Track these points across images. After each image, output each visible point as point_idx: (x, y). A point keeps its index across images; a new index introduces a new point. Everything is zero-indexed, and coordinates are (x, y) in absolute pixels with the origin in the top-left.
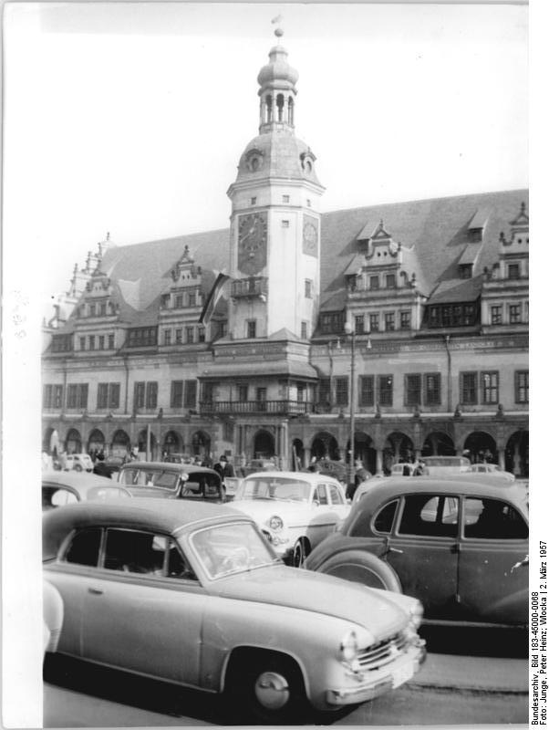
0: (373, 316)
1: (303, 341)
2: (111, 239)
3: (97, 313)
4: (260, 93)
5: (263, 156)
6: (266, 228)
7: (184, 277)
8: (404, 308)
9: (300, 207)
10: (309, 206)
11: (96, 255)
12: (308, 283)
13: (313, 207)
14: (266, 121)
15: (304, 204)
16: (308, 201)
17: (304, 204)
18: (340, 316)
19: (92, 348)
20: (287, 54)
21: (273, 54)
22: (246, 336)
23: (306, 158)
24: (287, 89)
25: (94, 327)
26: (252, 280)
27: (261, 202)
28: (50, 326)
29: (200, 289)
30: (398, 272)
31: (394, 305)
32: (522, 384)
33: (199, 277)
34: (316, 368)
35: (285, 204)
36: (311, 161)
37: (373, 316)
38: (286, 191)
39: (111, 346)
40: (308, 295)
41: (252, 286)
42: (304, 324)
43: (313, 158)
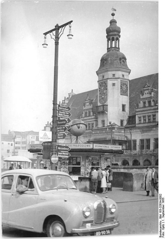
0: (144, 117)
4: (107, 37)
6: (107, 87)
7: (87, 105)
9: (119, 78)
10: (124, 77)
11: (68, 98)
12: (124, 106)
13: (125, 77)
14: (109, 47)
15: (121, 77)
16: (123, 75)
18: (134, 117)
20: (116, 22)
21: (111, 22)
22: (102, 126)
23: (123, 59)
24: (115, 35)
26: (103, 106)
27: (105, 78)
29: (92, 110)
31: (150, 113)
33: (92, 105)
34: (126, 137)
36: (124, 60)
37: (144, 117)
38: (114, 72)
40: (123, 110)
41: (103, 108)
42: (122, 122)
43: (125, 59)
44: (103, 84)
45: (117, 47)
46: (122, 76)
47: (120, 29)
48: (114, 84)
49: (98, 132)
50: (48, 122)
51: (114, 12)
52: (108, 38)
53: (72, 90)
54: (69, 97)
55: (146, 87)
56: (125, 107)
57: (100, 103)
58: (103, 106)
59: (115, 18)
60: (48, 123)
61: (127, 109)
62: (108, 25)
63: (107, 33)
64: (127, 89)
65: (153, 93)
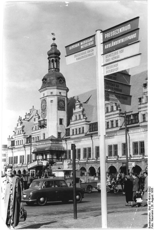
0: (76, 129)
1: (59, 139)
2: (34, 108)
3: (19, 133)
8: (83, 126)
11: (29, 114)
12: (61, 121)
15: (59, 94)
17: (59, 94)
19: (19, 145)
20: (56, 46)
21: (52, 46)
25: (18, 138)
26: (44, 120)
28: (12, 138)
32: (98, 149)
38: (51, 91)
39: (22, 144)
42: (59, 134)
44: (44, 101)
45: (56, 67)
46: (59, 93)
47: (59, 51)
48: (52, 100)
49: (41, 144)
50: (9, 136)
52: (49, 59)
53: (33, 106)
54: (30, 113)
55: (77, 103)
56: (63, 121)
57: (42, 118)
58: (44, 120)
59: (55, 42)
60: (9, 137)
61: (65, 122)
62: (49, 48)
63: (49, 55)
64: (65, 105)
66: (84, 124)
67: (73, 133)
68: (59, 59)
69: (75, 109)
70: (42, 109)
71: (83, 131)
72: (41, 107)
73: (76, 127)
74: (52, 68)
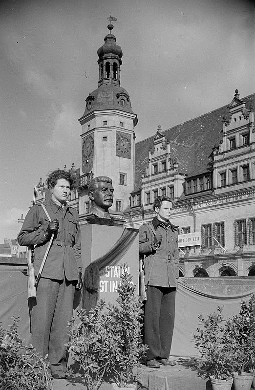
5: (93, 99)
13: (126, 126)
15: (119, 125)
21: (105, 39)
30: (168, 158)
31: (165, 182)
35: (104, 126)
36: (125, 99)
38: (105, 118)
43: (128, 97)
47: (120, 49)
48: (106, 137)
51: (113, 23)
52: (100, 64)
59: (113, 32)
64: (130, 148)
65: (169, 147)
66: (173, 180)
67: (149, 199)
68: (121, 63)
69: (152, 153)
70: (84, 156)
71: (173, 193)
72: (83, 151)
73: (155, 188)
74: (106, 77)
